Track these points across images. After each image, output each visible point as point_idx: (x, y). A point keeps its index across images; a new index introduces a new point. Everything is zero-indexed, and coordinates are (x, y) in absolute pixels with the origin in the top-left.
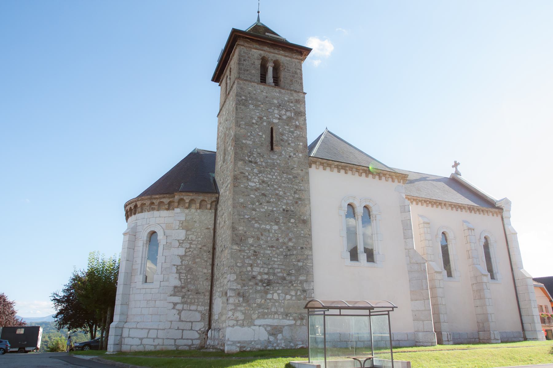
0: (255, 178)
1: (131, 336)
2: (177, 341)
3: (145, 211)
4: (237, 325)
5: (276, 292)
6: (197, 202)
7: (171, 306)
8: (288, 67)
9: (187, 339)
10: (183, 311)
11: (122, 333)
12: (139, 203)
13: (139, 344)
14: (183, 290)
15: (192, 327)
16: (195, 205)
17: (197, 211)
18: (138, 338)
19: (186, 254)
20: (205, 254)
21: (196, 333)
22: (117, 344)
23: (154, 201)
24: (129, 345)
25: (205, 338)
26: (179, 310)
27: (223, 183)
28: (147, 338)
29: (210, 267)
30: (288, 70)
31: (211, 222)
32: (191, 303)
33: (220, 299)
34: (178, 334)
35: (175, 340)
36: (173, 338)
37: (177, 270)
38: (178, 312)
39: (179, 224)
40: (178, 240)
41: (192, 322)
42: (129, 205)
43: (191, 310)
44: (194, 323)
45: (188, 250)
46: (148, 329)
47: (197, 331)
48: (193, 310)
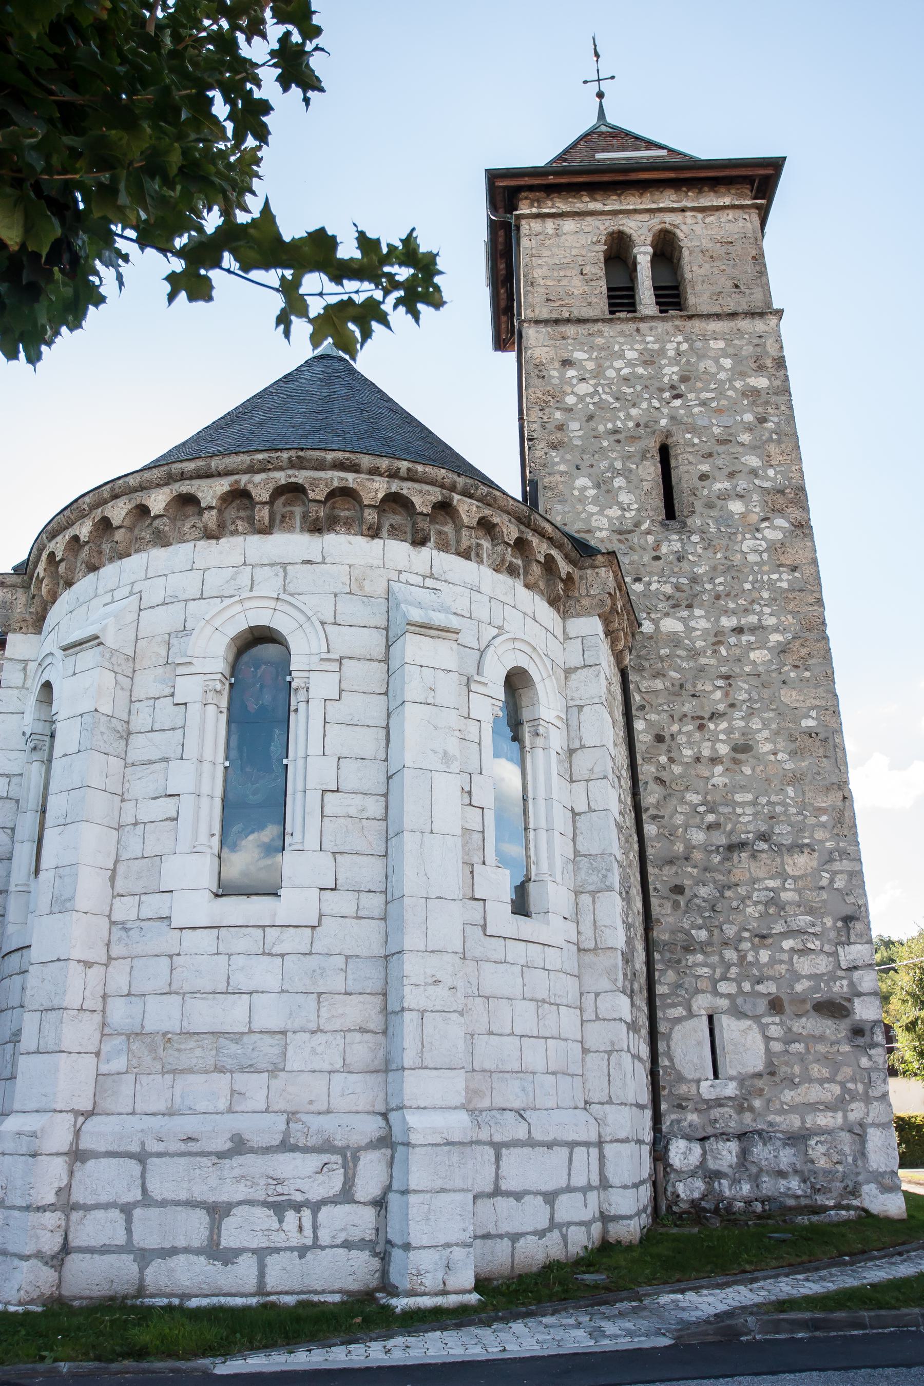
1: (511, 1188)
13: (545, 1224)
24: (501, 1236)
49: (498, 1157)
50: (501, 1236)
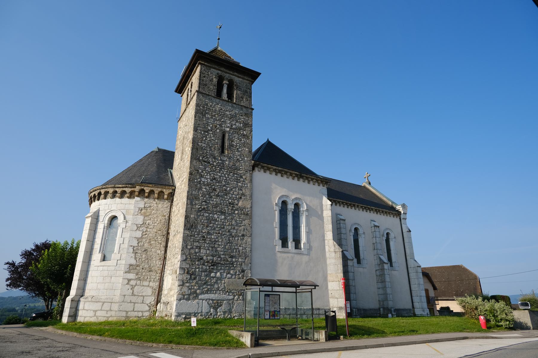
0: (207, 175)
2: (129, 313)
3: (108, 198)
4: (184, 299)
5: (219, 271)
6: (155, 193)
7: (126, 281)
8: (240, 86)
9: (138, 311)
10: (136, 287)
11: (77, 305)
12: (103, 191)
14: (138, 268)
15: (143, 300)
16: (153, 195)
17: (155, 200)
18: (92, 310)
19: (143, 237)
20: (160, 237)
21: (147, 306)
22: (72, 316)
23: (117, 190)
24: (83, 317)
25: (154, 311)
26: (132, 285)
27: (179, 178)
28: (101, 310)
29: (163, 249)
30: (240, 89)
31: (167, 210)
32: (144, 280)
33: (171, 276)
34: (130, 307)
35: (127, 312)
36: (125, 310)
37: (134, 250)
38: (131, 287)
39: (139, 210)
40: (136, 225)
41: (144, 296)
42: (93, 192)
43: (143, 286)
44: (145, 297)
45: (145, 233)
46: (102, 302)
47: (147, 305)
48: (145, 286)
49: (85, 303)
50: (83, 317)
